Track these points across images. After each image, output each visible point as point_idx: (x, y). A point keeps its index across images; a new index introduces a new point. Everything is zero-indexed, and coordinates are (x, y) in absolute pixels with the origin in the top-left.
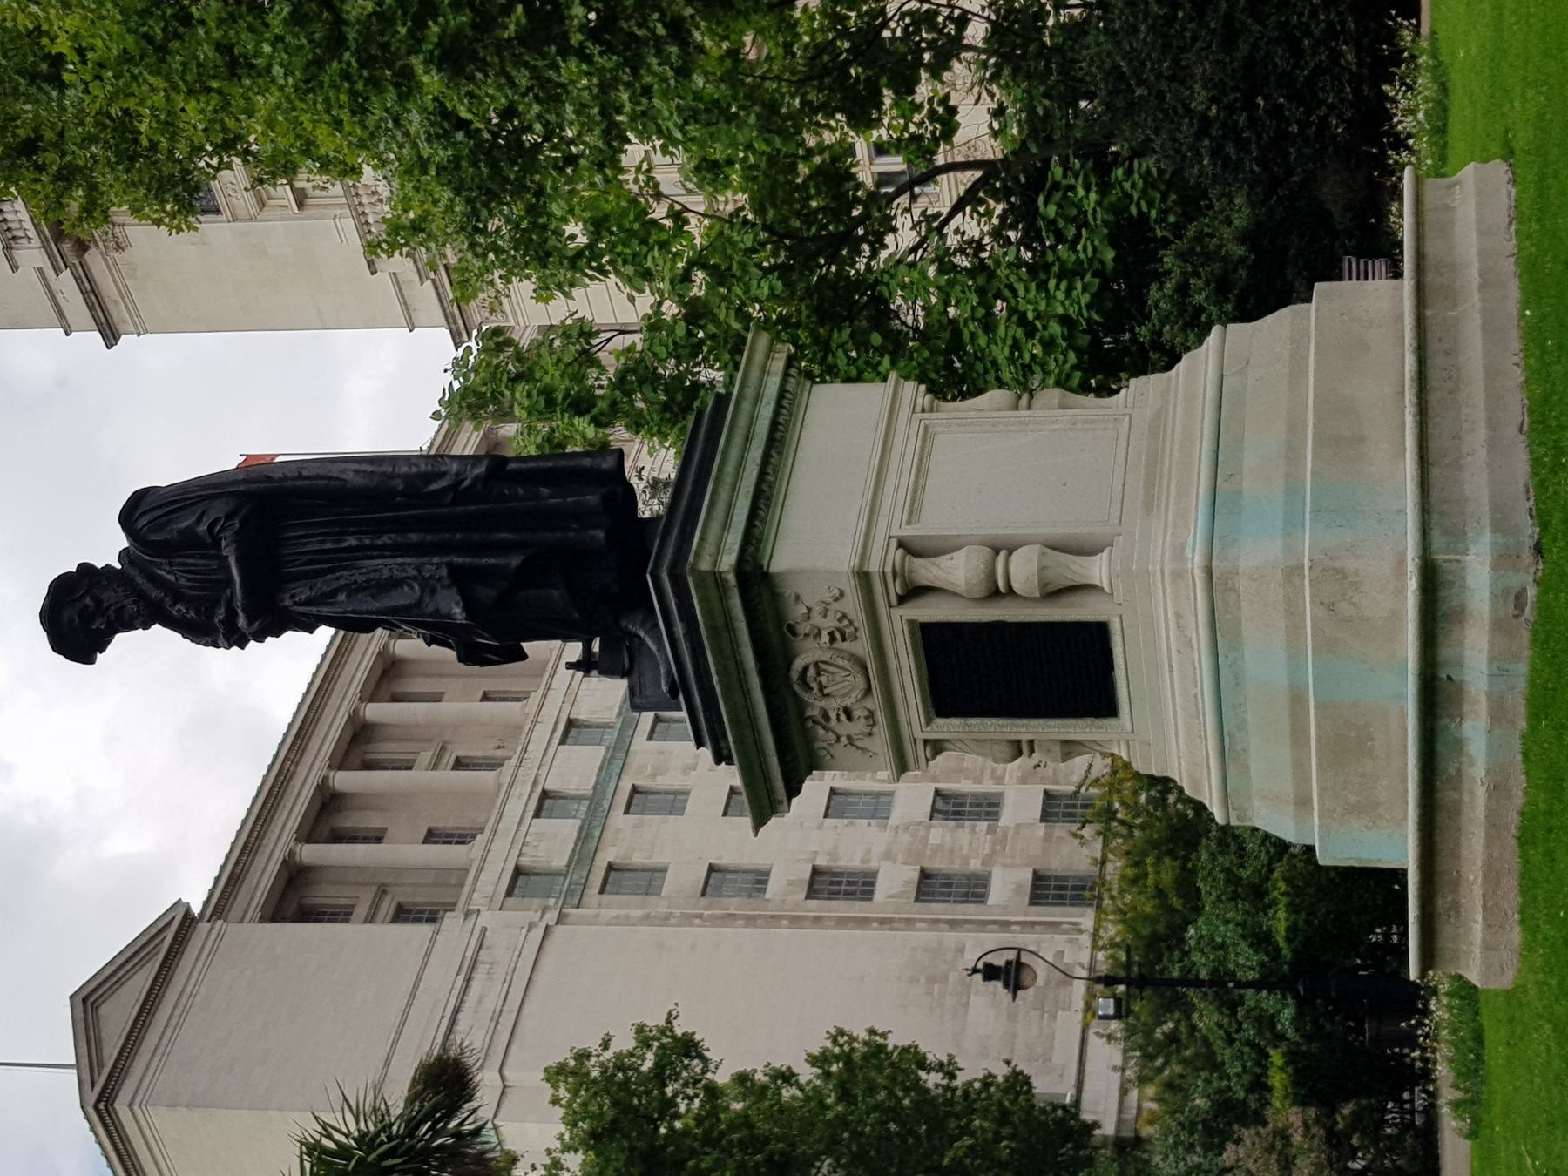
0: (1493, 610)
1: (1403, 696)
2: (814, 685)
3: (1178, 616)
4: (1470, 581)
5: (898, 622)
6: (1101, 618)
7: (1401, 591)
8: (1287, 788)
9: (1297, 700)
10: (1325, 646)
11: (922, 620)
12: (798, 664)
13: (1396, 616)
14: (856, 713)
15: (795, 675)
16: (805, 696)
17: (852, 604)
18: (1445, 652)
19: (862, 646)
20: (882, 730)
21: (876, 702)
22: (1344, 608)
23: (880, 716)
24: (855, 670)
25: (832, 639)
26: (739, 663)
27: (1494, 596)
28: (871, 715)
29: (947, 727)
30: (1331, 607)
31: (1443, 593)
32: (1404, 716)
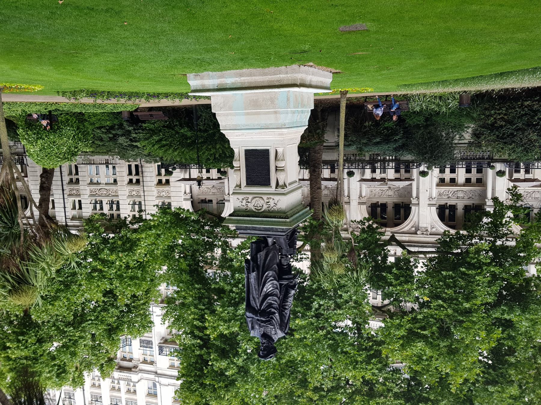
0: (199, 80)
1: (242, 94)
2: (260, 208)
3: (237, 136)
4: (195, 84)
5: (244, 189)
6: (244, 151)
7: (217, 96)
8: (273, 116)
9: (248, 114)
10: (230, 109)
11: (245, 184)
12: (254, 210)
13: (223, 96)
14: (268, 201)
15: (257, 211)
16: (263, 210)
17: (241, 197)
18: (211, 88)
19: (251, 197)
20: (271, 196)
21: (265, 197)
22: (222, 105)
23: (269, 196)
24: (255, 200)
25: (248, 202)
26: (248, 220)
27: (196, 80)
28: (268, 198)
29: (273, 183)
30: (221, 108)
31: (198, 88)
32: (247, 94)
